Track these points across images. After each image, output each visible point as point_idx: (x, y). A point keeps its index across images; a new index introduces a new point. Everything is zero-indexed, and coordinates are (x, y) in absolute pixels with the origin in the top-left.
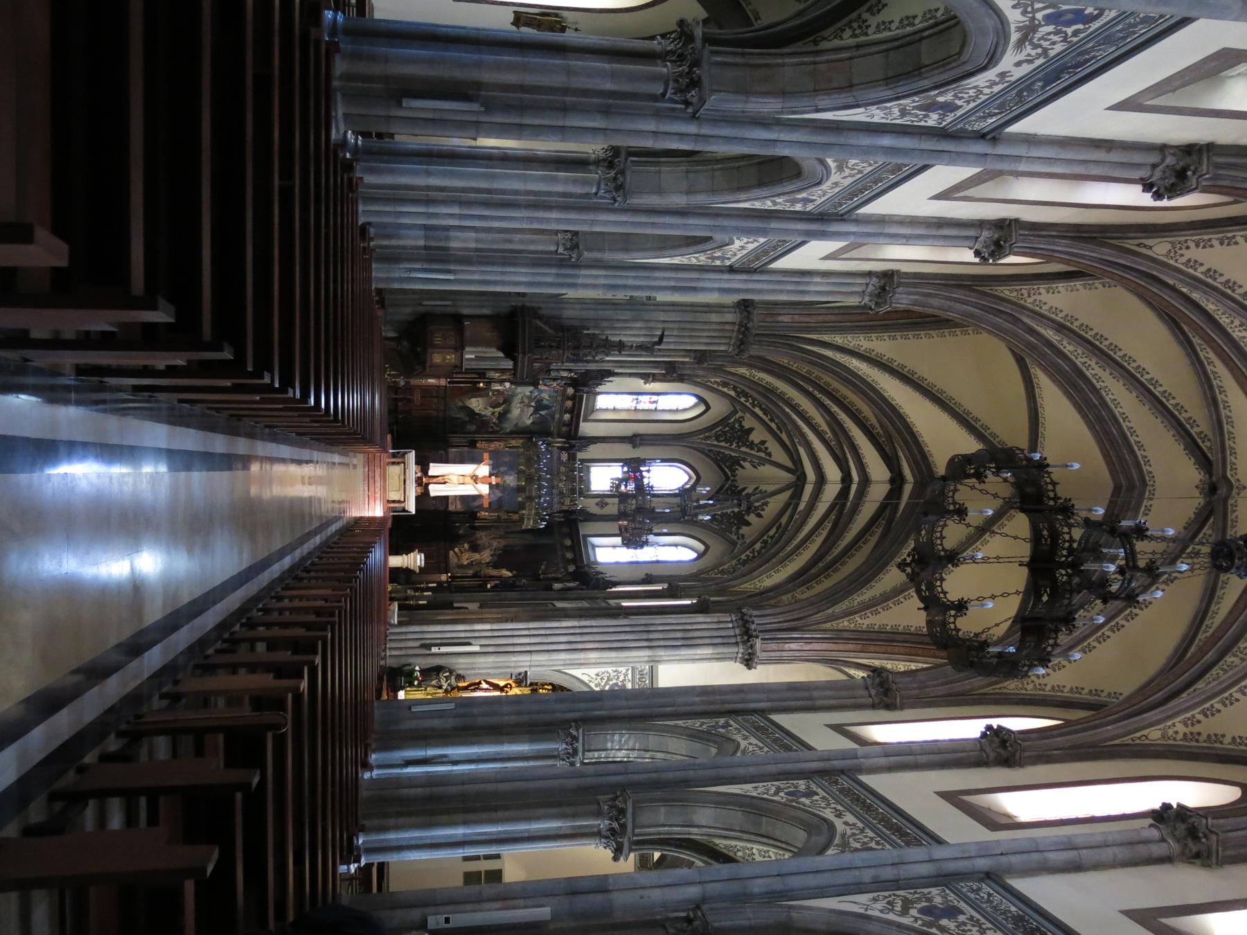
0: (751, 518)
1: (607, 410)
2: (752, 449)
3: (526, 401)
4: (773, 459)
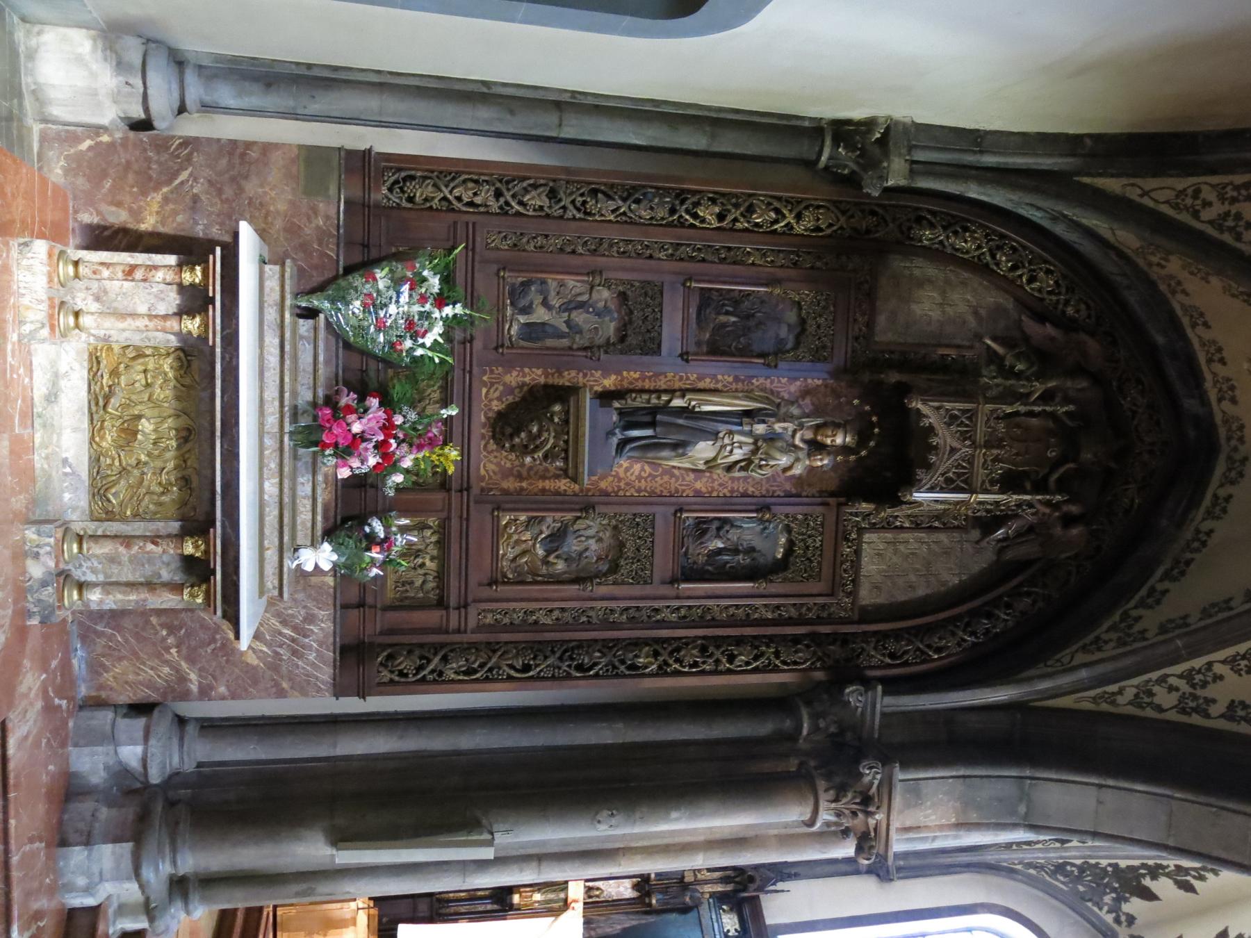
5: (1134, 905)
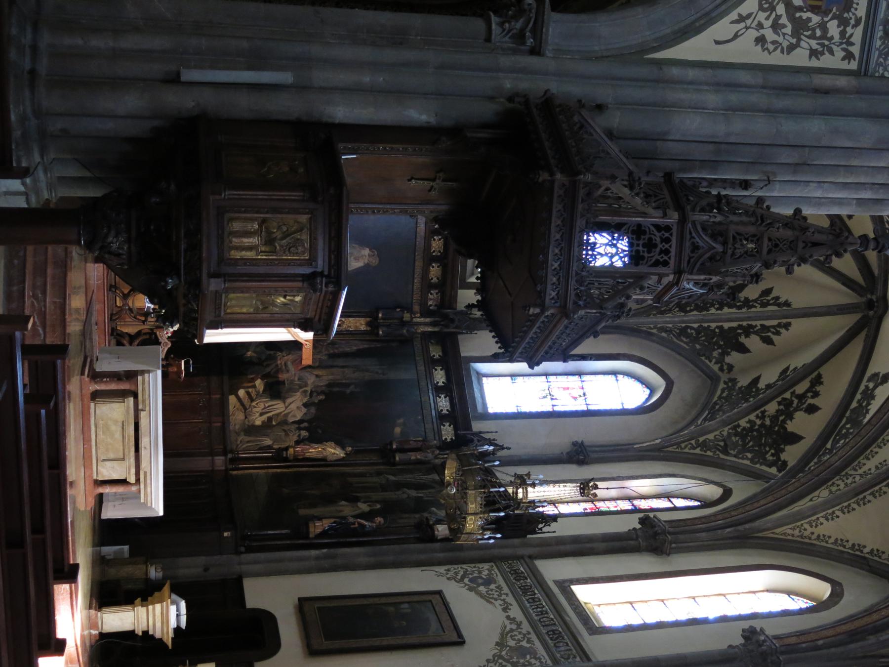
0: (753, 342)
5: (734, 358)
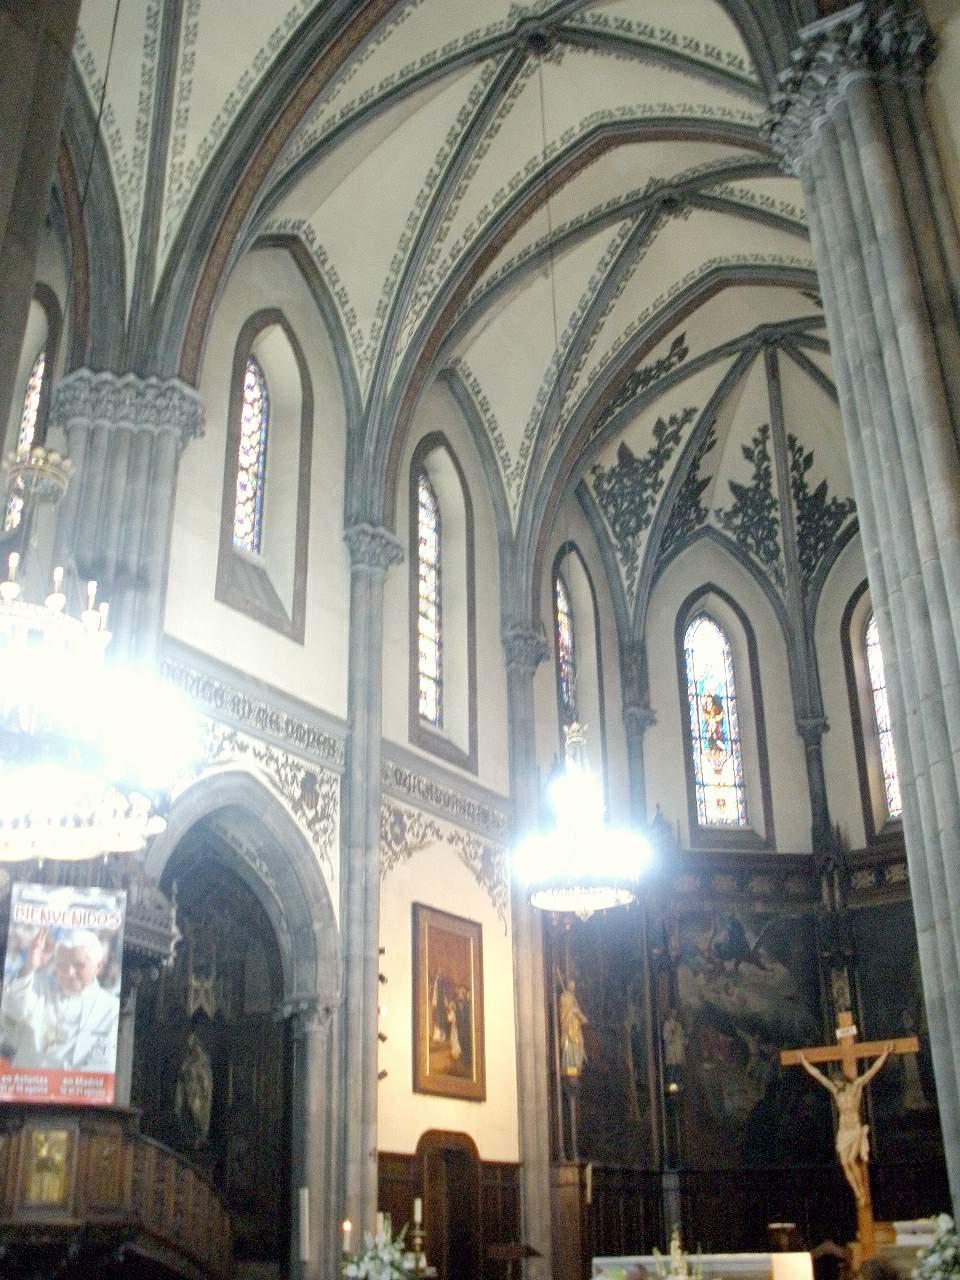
1: (745, 802)
2: (768, 474)
3: (722, 981)
4: (766, 418)
